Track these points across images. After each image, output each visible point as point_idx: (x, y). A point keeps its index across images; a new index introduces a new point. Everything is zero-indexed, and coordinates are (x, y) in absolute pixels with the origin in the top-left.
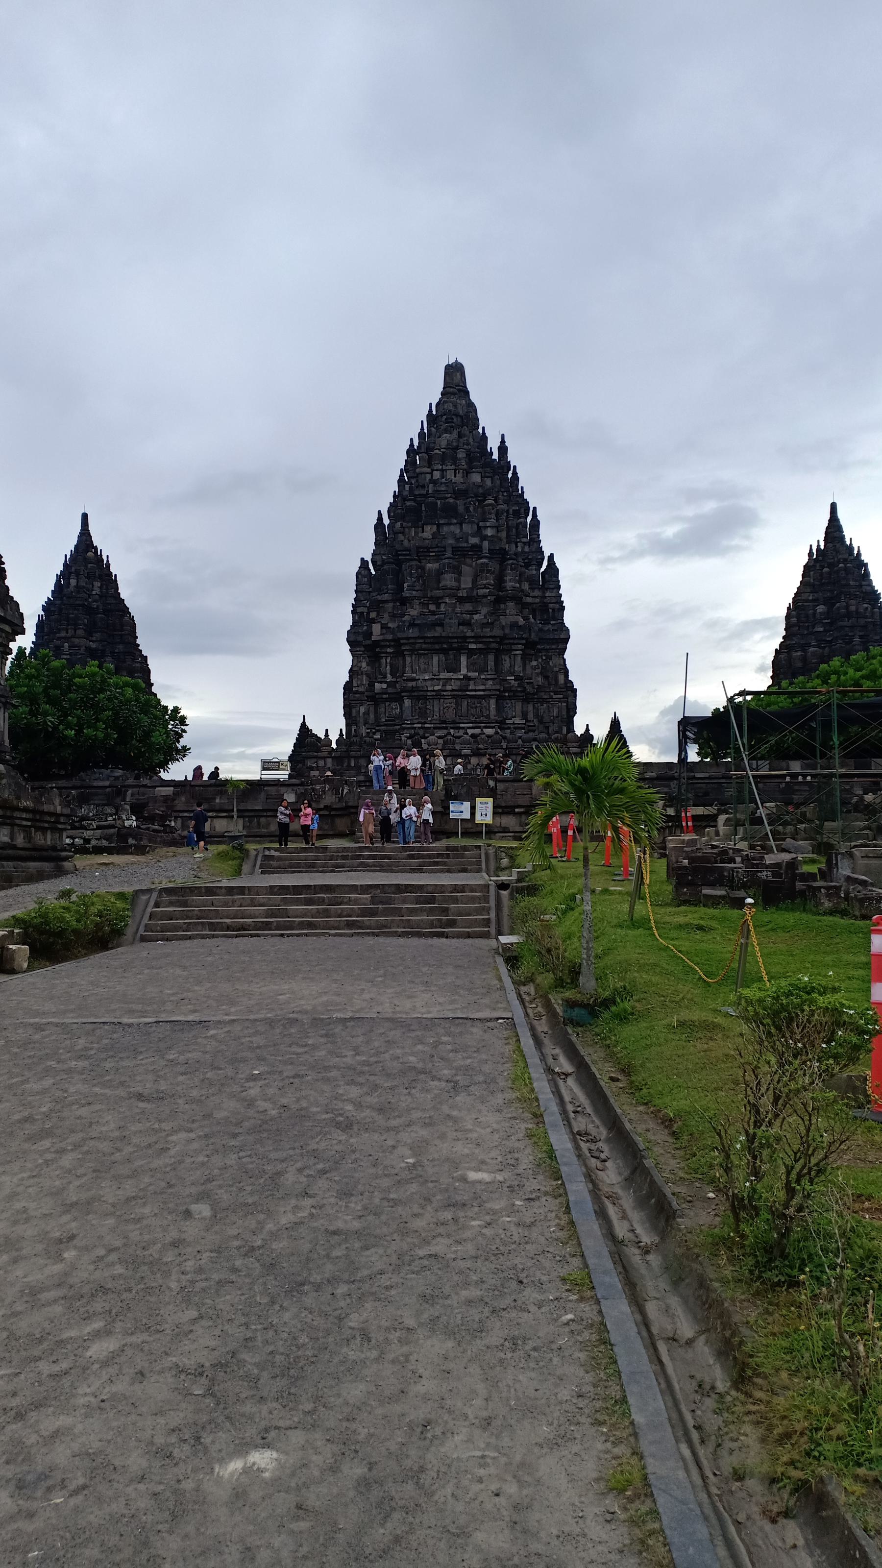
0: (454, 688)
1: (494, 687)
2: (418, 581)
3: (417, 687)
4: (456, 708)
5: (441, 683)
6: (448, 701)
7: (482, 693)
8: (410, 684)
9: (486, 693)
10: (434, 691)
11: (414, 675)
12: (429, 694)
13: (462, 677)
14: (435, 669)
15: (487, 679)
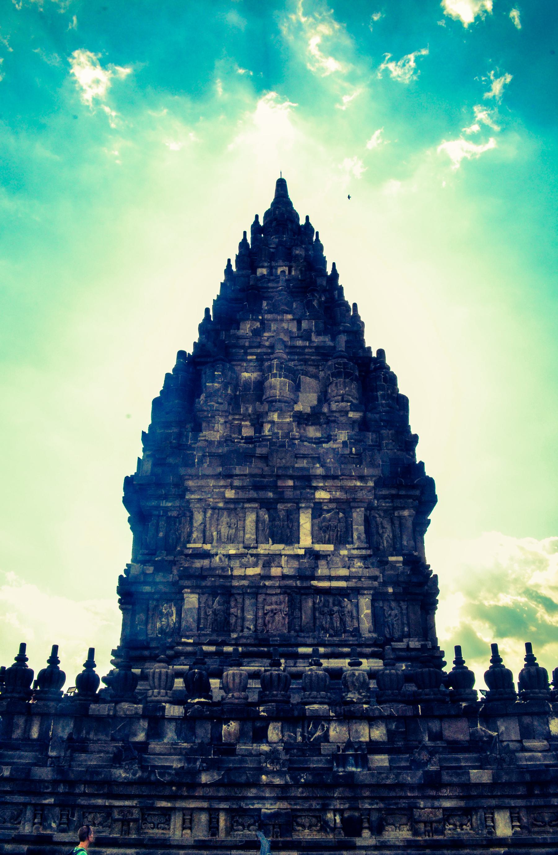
0: (286, 571)
1: (367, 573)
2: (226, 388)
3: (211, 569)
4: (290, 615)
5: (261, 563)
6: (274, 599)
7: (342, 584)
8: (198, 564)
9: (352, 584)
10: (245, 577)
11: (208, 547)
12: (235, 583)
13: (302, 552)
14: (250, 535)
15: (351, 558)
